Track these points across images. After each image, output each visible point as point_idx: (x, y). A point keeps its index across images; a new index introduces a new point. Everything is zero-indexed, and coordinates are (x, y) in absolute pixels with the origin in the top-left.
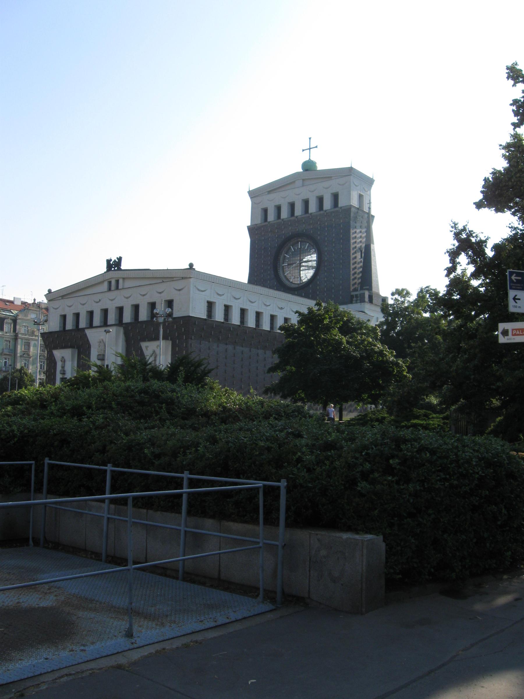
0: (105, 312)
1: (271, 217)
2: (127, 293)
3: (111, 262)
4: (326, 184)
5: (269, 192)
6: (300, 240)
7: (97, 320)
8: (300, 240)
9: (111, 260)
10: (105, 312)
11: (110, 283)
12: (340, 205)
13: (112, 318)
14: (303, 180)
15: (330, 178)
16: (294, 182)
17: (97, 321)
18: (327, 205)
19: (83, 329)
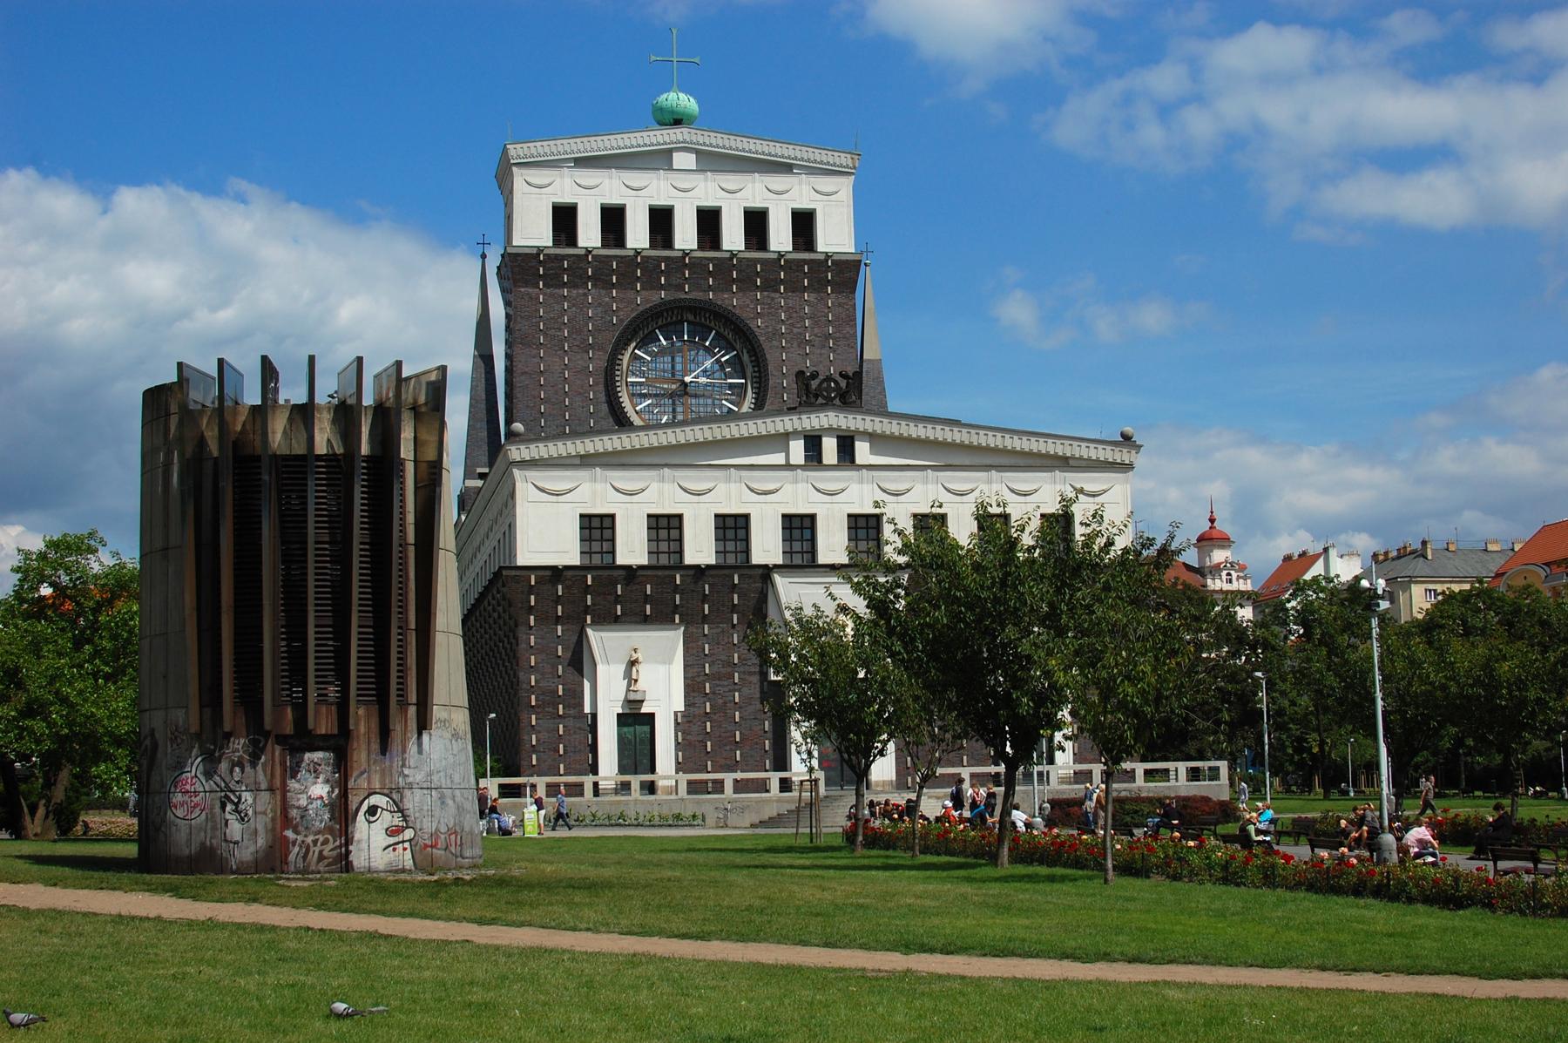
0: (800, 528)
1: (589, 234)
2: (895, 481)
3: (814, 384)
4: (778, 181)
5: (582, 162)
6: (691, 317)
7: (766, 547)
8: (691, 317)
9: (814, 376)
10: (800, 528)
11: (813, 444)
12: (822, 246)
13: (833, 545)
14: (697, 152)
15: (786, 168)
16: (670, 151)
17: (766, 547)
18: (780, 237)
19: (767, 571)
